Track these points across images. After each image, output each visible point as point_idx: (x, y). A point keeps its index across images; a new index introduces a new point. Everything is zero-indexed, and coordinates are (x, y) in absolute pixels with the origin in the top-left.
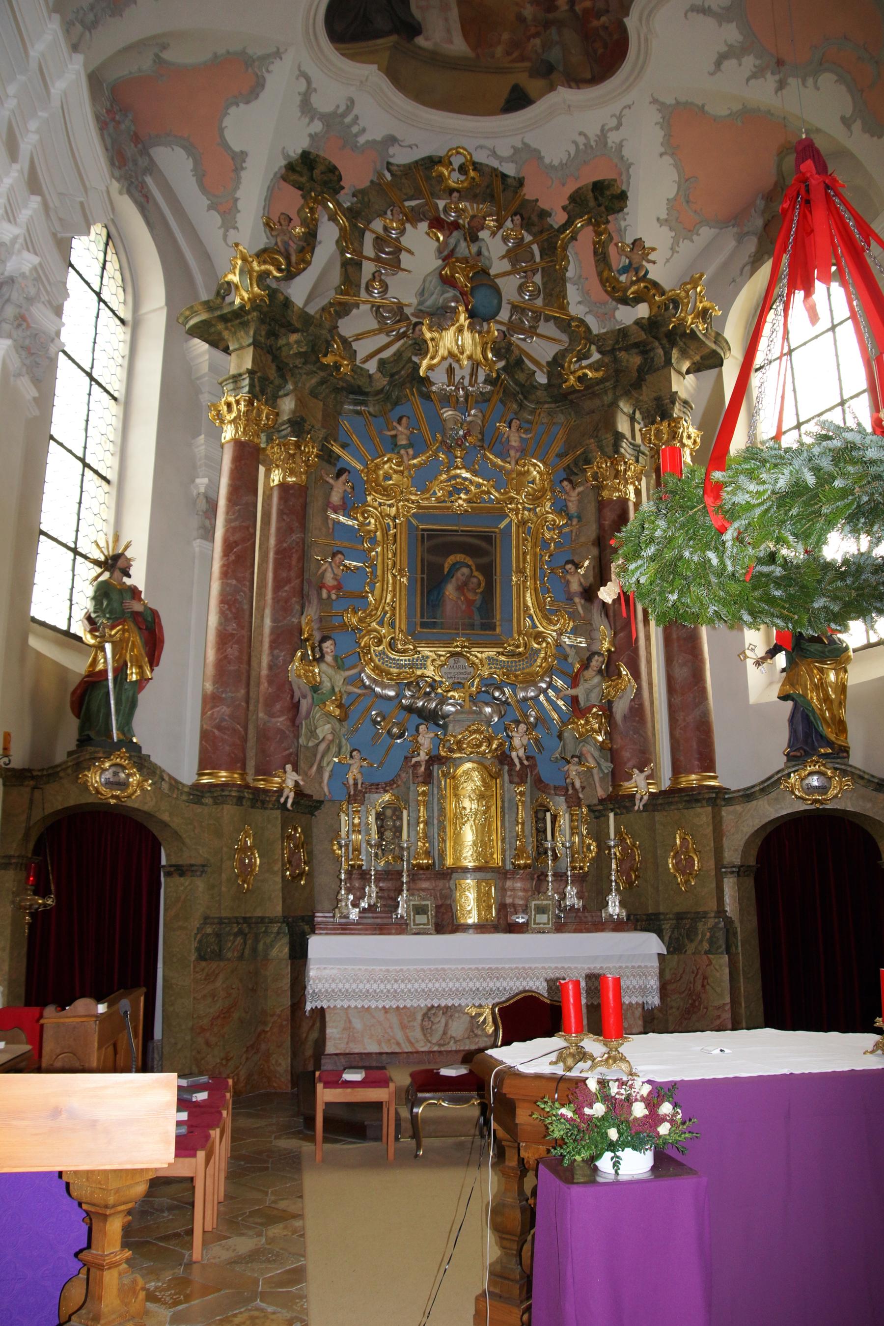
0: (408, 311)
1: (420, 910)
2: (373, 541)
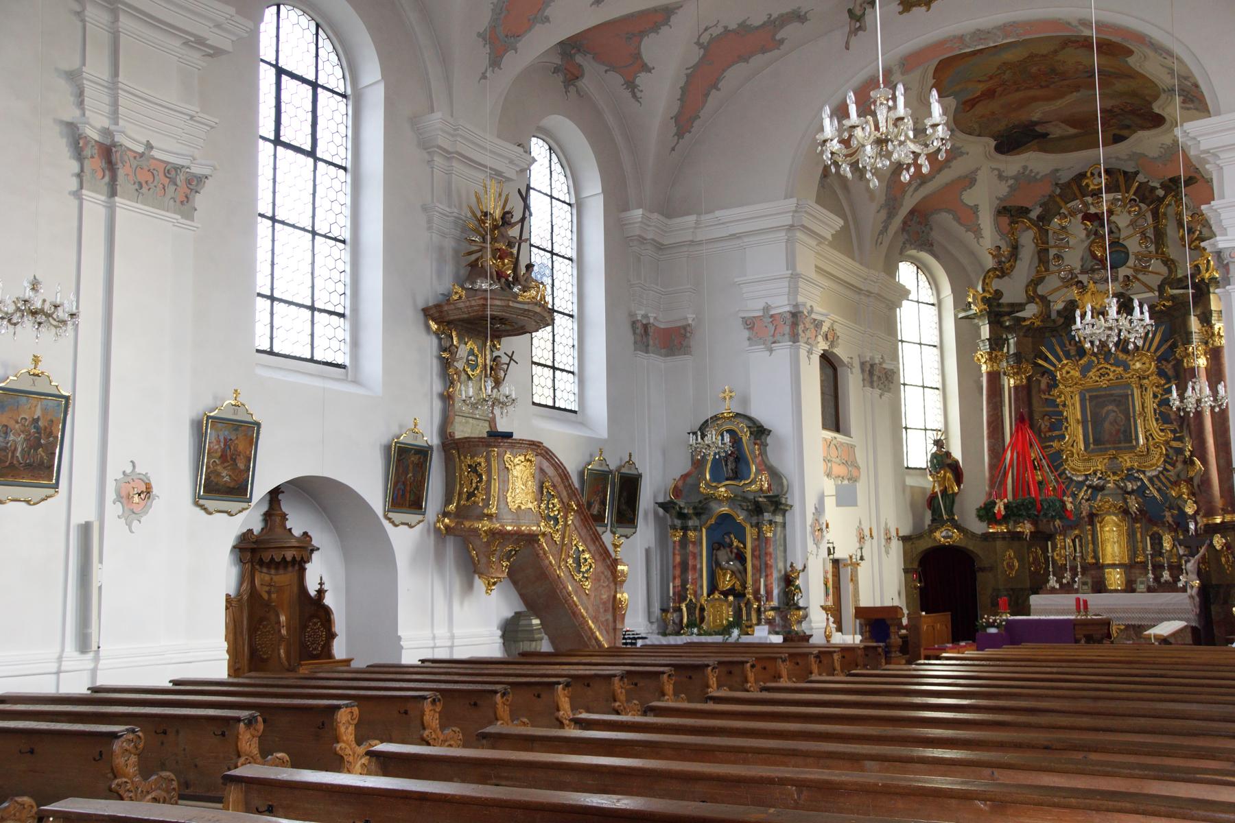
0: (1077, 271)
1: (1084, 583)
2: (1064, 405)
